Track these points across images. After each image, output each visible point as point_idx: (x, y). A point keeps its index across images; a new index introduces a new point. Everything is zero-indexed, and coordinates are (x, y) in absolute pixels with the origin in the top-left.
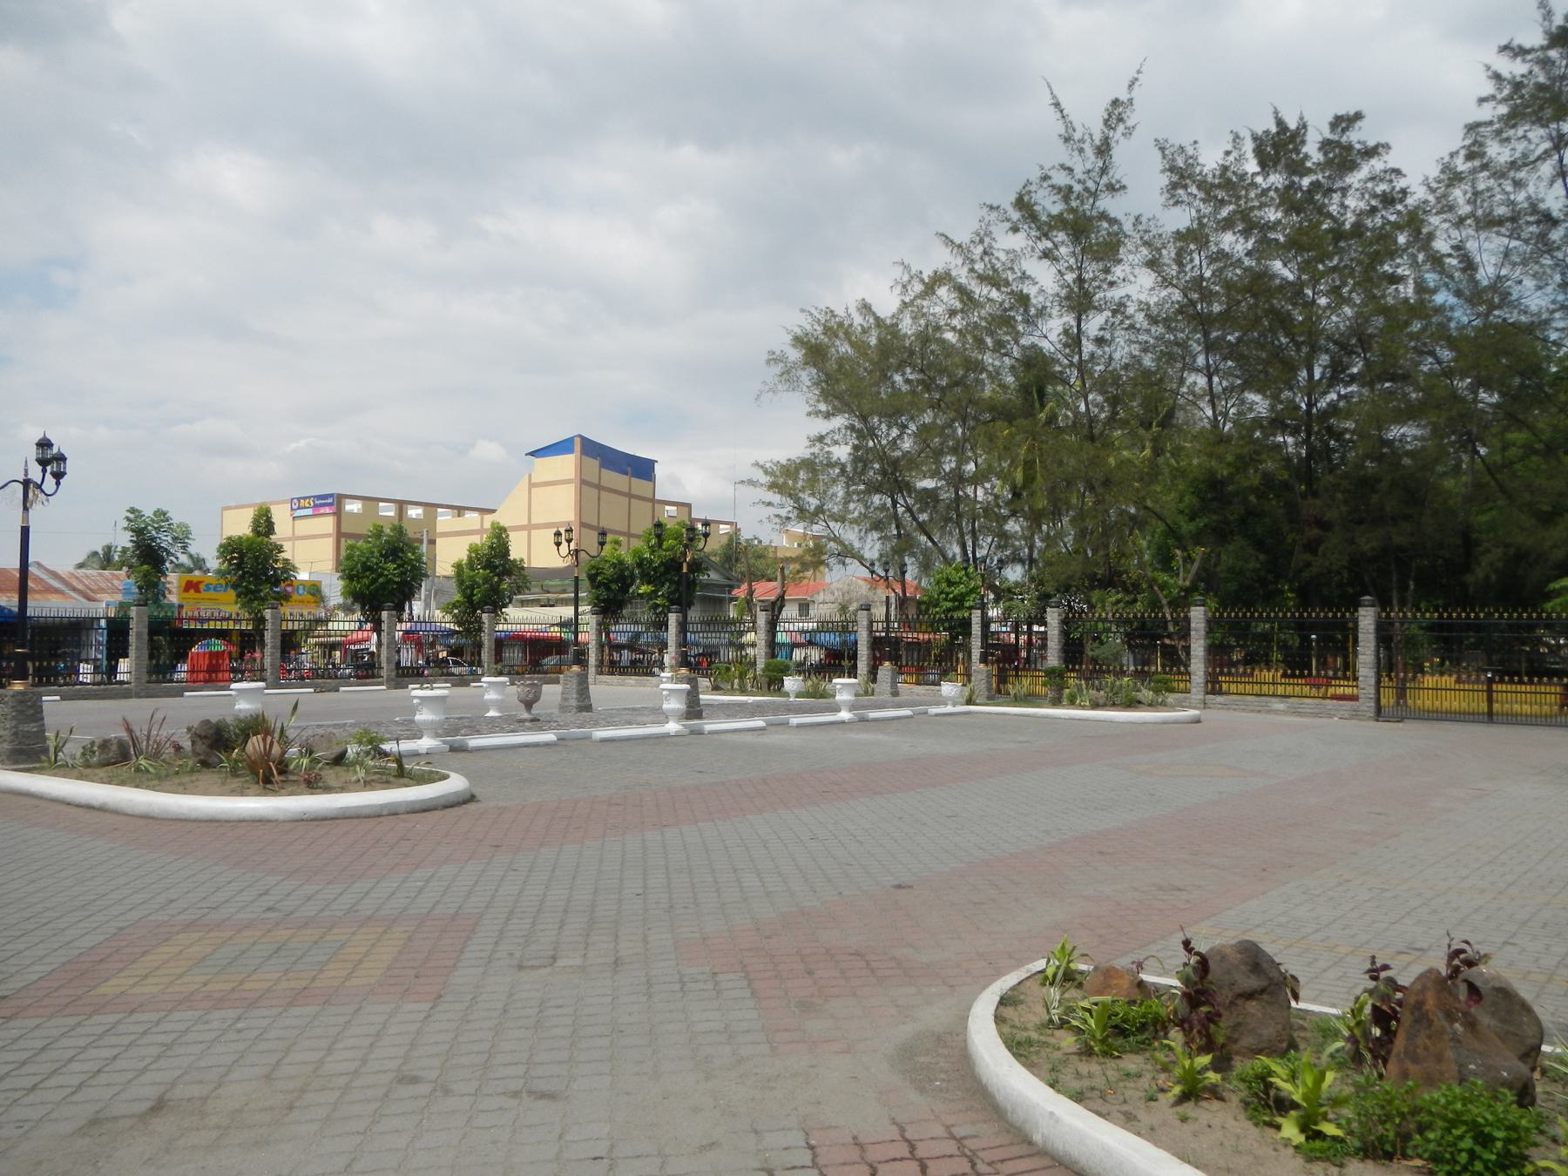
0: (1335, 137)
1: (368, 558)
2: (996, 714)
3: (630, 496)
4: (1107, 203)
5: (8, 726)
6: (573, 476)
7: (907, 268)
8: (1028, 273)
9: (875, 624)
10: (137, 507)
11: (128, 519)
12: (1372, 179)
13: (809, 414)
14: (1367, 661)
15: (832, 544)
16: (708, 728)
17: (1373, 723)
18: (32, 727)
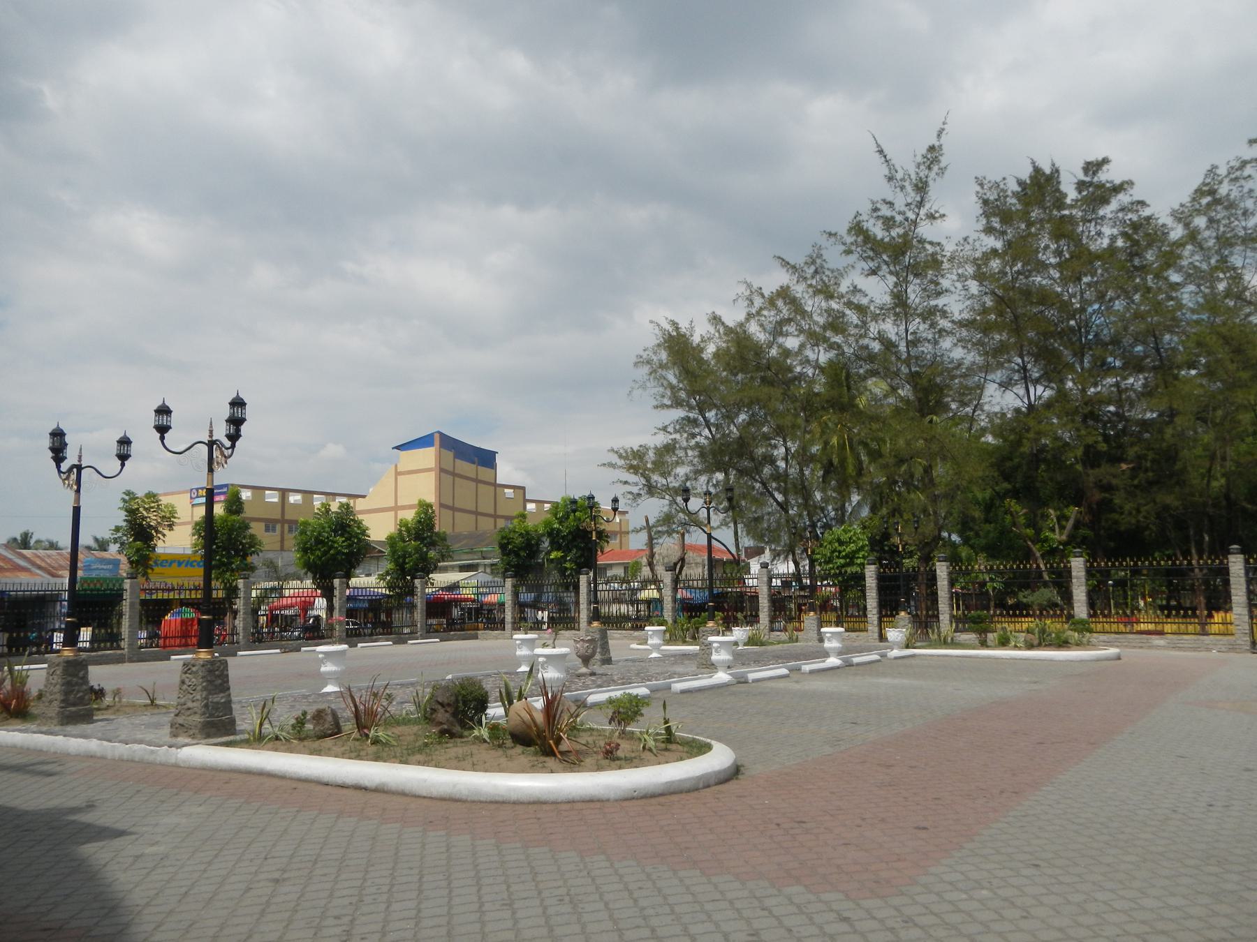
0: (1088, 179)
1: (320, 534)
2: (938, 656)
3: (477, 481)
4: (926, 230)
5: (199, 697)
6: (434, 466)
7: (749, 286)
8: (859, 287)
9: (774, 580)
10: (133, 490)
11: (124, 500)
12: (1122, 210)
13: (656, 407)
14: (1240, 601)
15: (681, 515)
16: (751, 676)
17: (1250, 655)
18: (219, 698)
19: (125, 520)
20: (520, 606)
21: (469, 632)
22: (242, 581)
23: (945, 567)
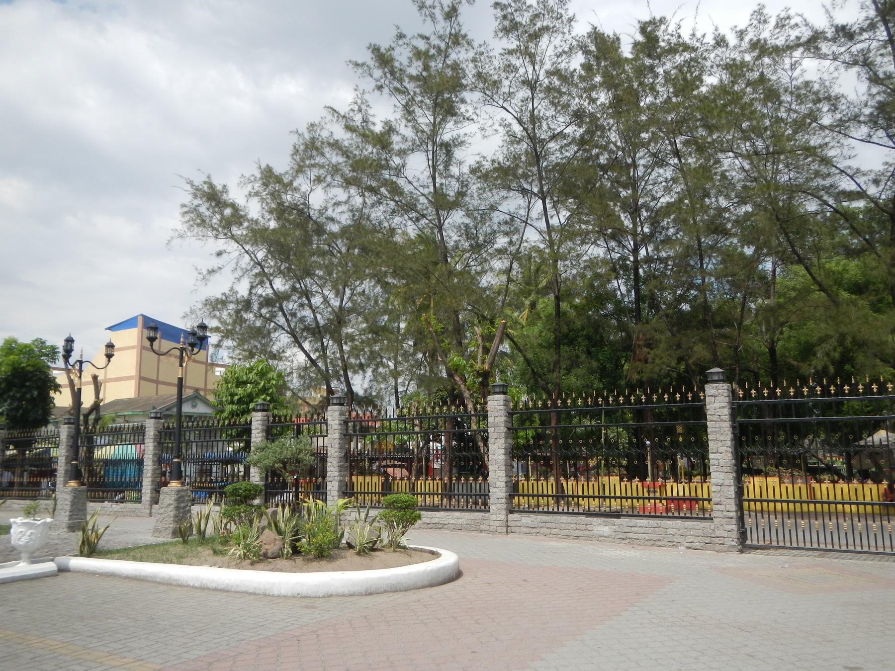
14: (722, 462)
23: (338, 413)
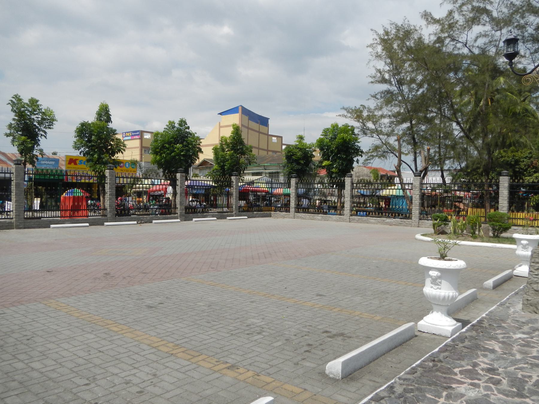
3: (259, 132)
19: (14, 119)
20: (299, 197)
21: (266, 212)
22: (108, 171)
